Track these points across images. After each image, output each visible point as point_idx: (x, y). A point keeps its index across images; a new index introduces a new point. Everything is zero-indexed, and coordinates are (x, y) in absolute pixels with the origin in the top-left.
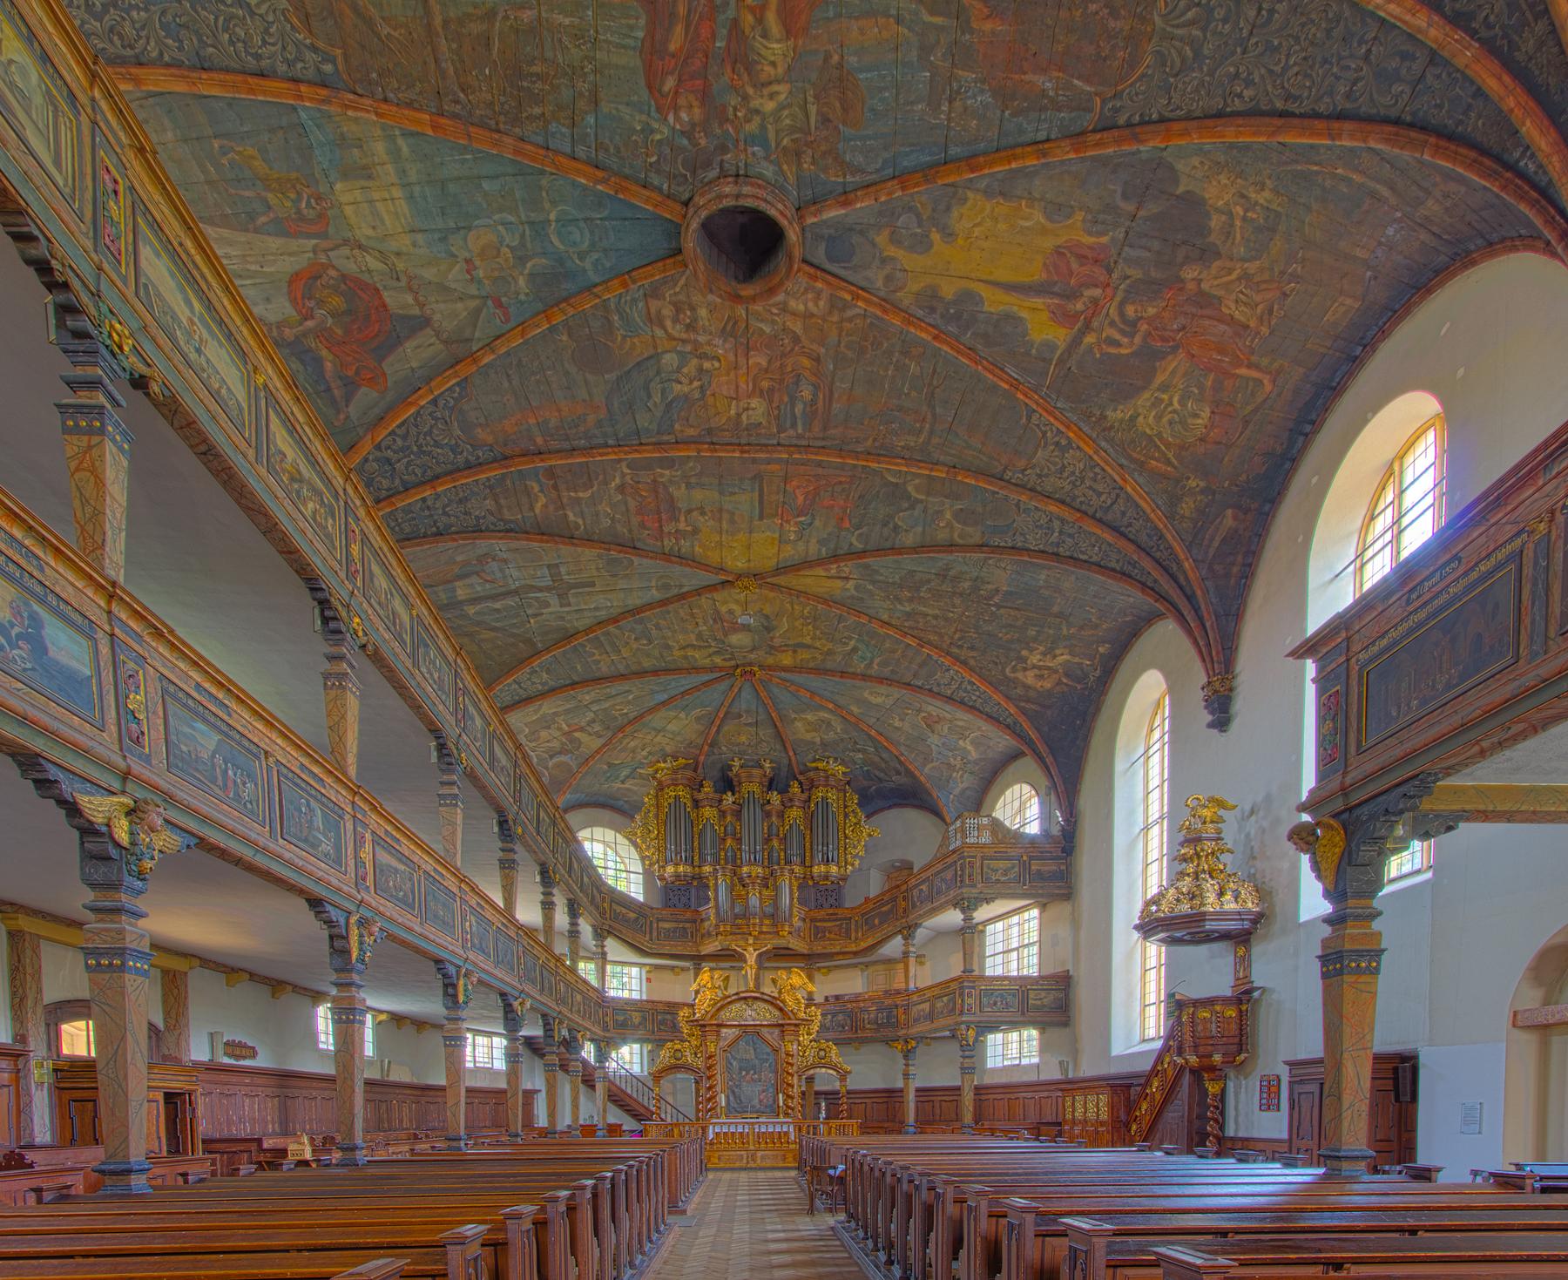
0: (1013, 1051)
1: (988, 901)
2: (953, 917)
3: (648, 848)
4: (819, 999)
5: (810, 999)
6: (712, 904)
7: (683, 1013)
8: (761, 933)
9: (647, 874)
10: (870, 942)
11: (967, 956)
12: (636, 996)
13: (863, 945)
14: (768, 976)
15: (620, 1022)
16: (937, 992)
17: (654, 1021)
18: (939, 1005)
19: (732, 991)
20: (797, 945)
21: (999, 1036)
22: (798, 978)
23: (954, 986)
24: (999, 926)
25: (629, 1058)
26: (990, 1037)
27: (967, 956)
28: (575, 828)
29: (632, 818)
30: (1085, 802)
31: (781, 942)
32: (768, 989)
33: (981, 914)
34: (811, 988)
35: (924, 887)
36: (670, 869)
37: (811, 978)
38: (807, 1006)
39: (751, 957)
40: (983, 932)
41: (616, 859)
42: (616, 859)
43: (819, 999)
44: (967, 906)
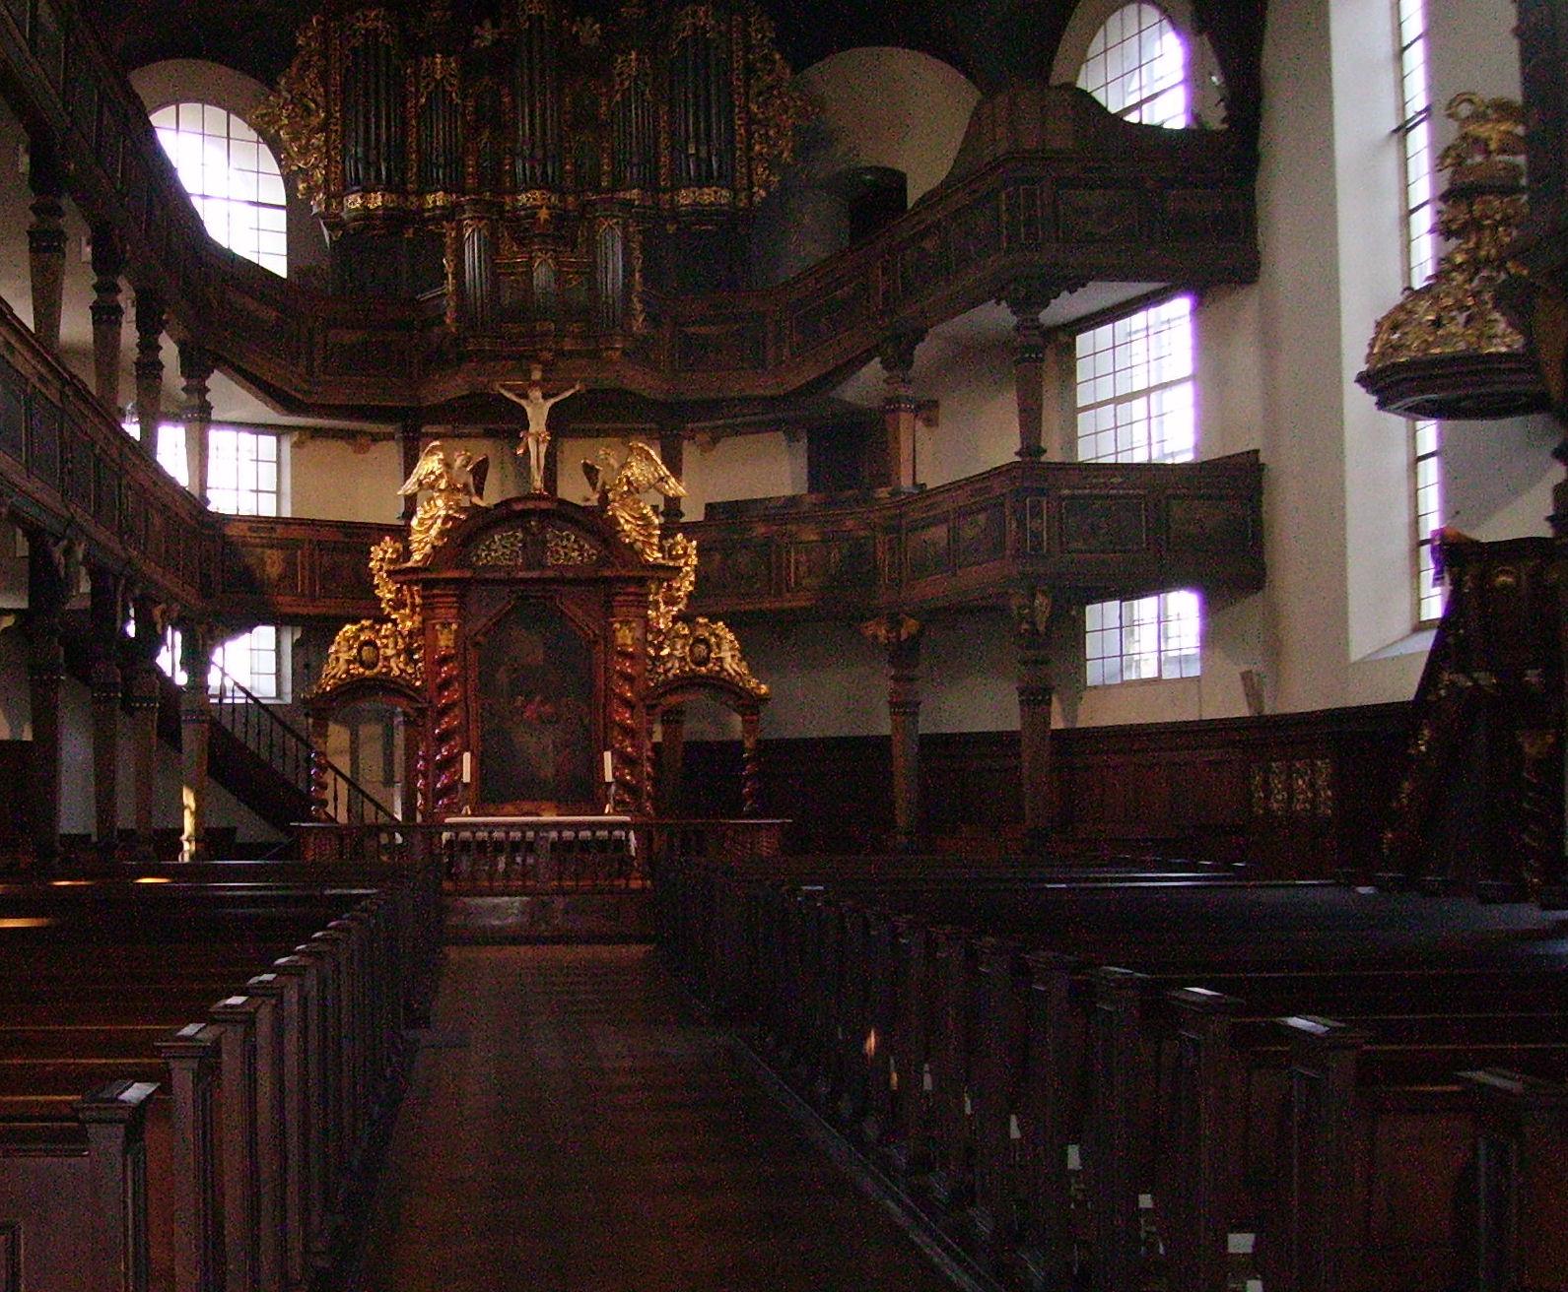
0: (1153, 641)
1: (1074, 284)
2: (997, 317)
3: (304, 152)
4: (693, 513)
5: (672, 508)
6: (450, 285)
7: (382, 552)
8: (560, 354)
9: (295, 209)
10: (810, 373)
11: (1031, 419)
12: (268, 509)
13: (795, 381)
14: (575, 453)
15: (228, 573)
16: (962, 499)
17: (303, 573)
18: (969, 532)
19: (490, 498)
20: (643, 382)
21: (1112, 607)
22: (643, 466)
23: (998, 487)
24: (1104, 332)
25: (249, 664)
26: (1093, 612)
27: (1031, 419)
28: (148, 105)
29: (272, 85)
30: (1275, 60)
31: (608, 379)
32: (574, 490)
33: (1063, 307)
34: (673, 487)
35: (928, 244)
36: (354, 202)
37: (675, 466)
38: (667, 531)
39: (538, 412)
40: (1071, 347)
41: (232, 185)
42: (232, 185)
43: (693, 513)
44: (1030, 297)
